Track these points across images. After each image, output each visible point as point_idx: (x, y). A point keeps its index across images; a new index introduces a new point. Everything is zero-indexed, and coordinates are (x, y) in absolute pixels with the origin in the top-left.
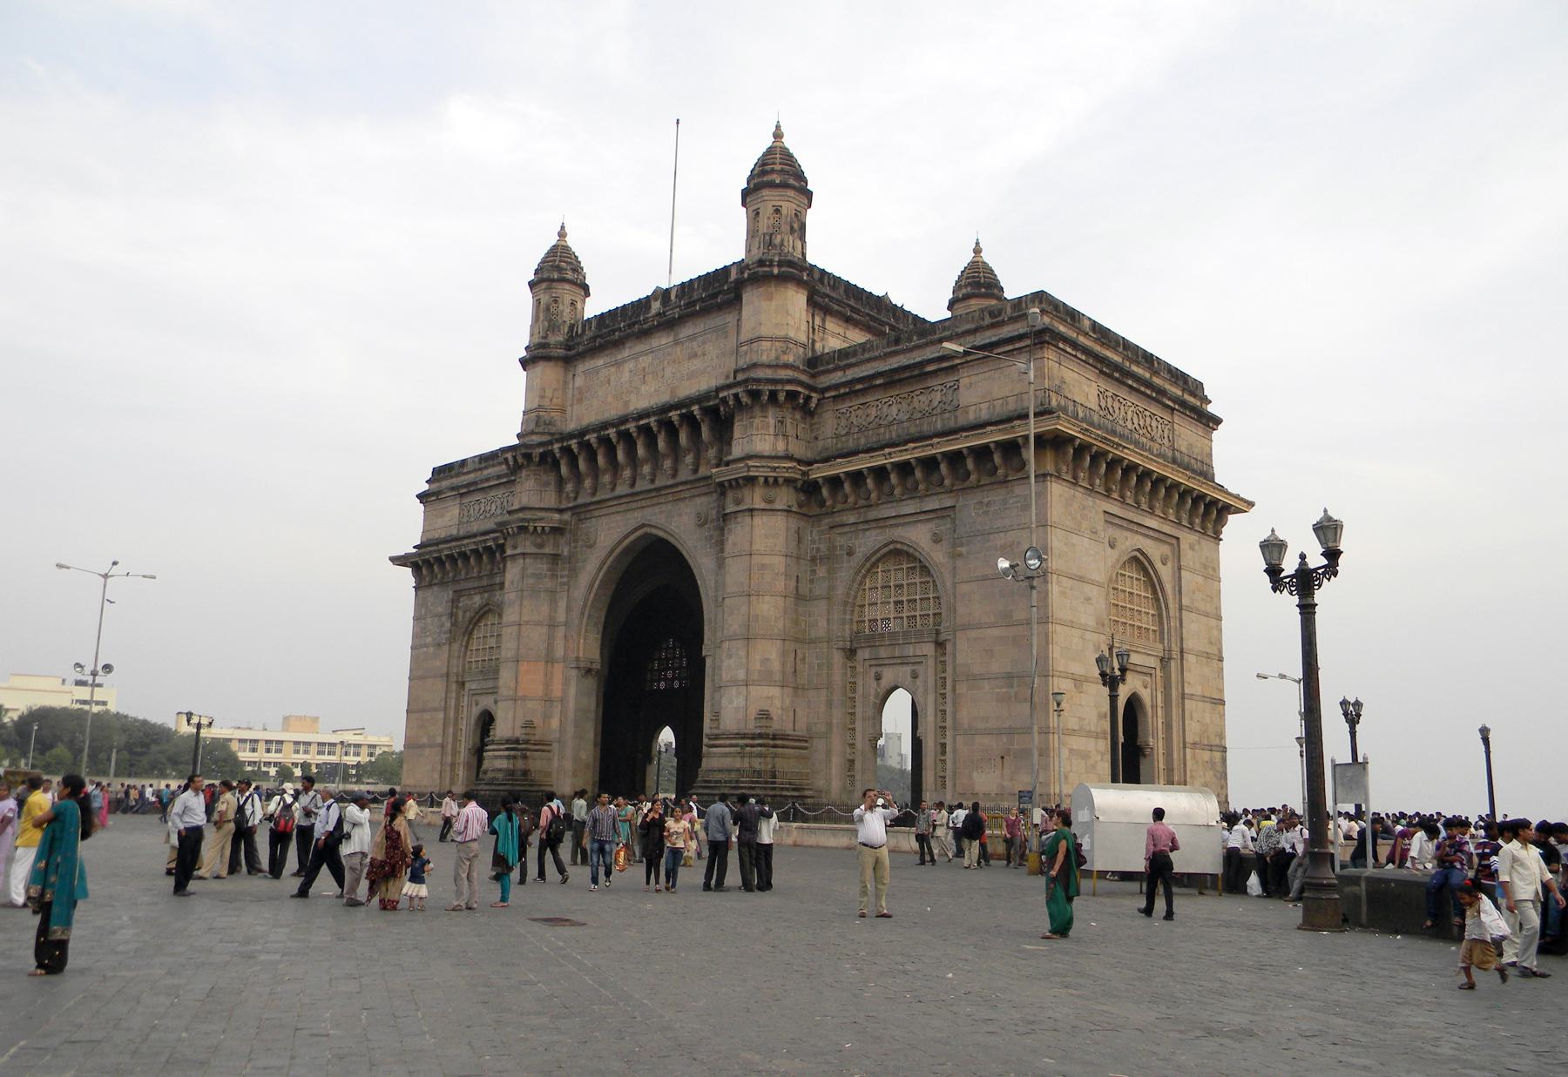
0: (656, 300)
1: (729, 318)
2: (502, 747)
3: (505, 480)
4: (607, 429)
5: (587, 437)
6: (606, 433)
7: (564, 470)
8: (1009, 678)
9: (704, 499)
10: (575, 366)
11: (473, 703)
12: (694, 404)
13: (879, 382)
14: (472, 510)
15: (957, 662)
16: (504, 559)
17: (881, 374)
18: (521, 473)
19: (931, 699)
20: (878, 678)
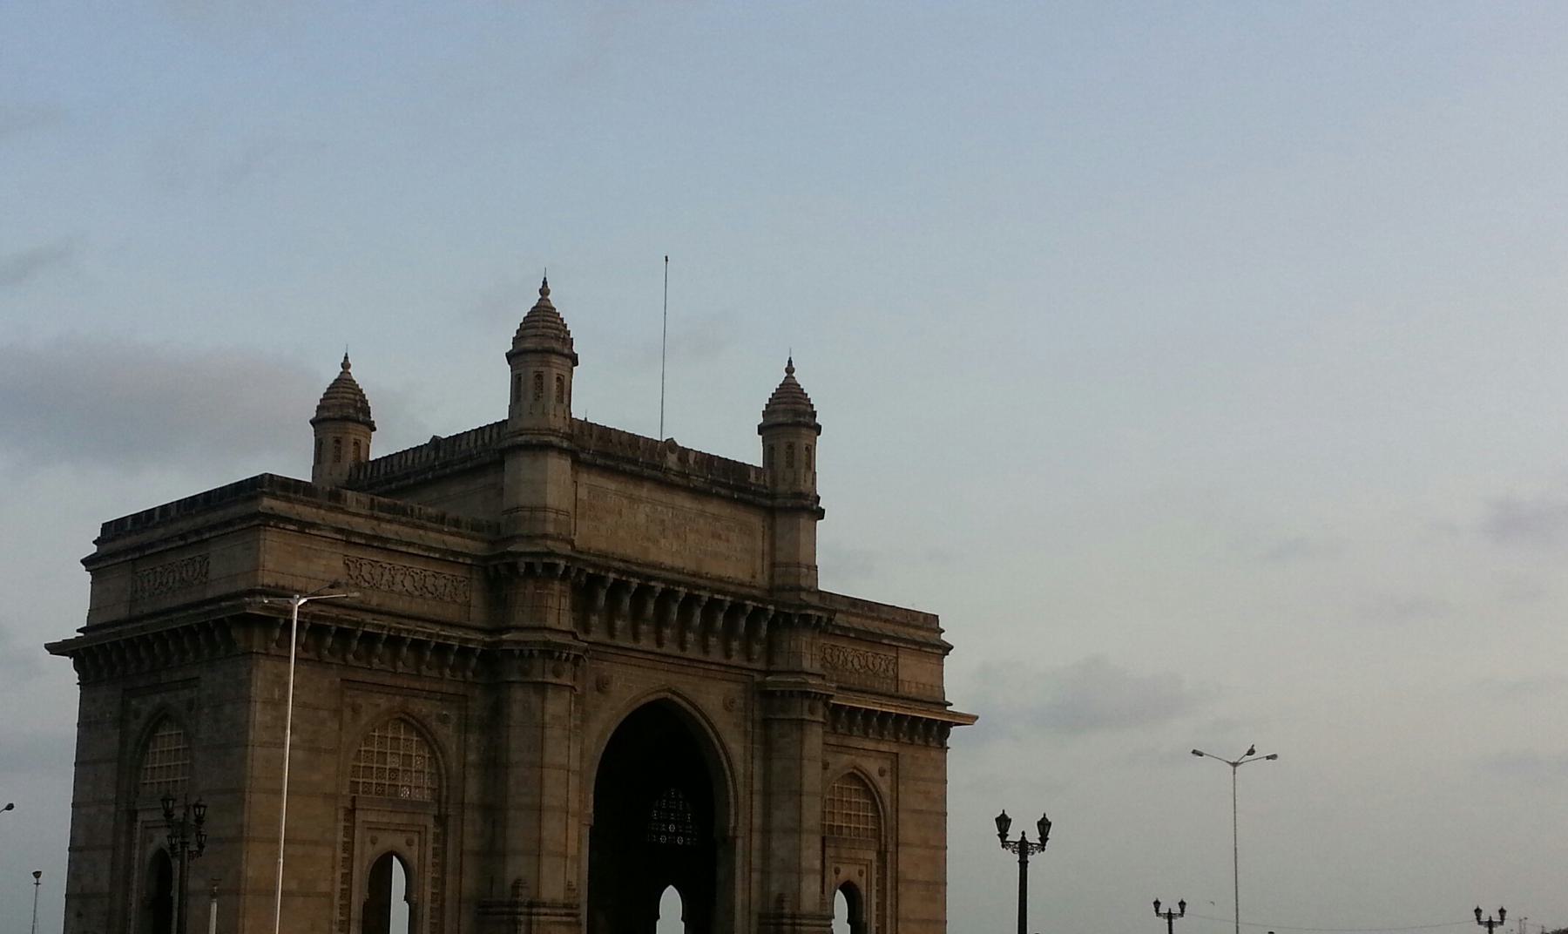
0: (672, 451)
1: (756, 521)
2: (558, 911)
3: (437, 556)
4: (679, 584)
5: (653, 583)
6: (677, 589)
7: (602, 600)
8: (928, 883)
9: (732, 686)
10: (577, 473)
11: (368, 839)
12: (770, 604)
13: (852, 635)
14: (366, 569)
15: (899, 869)
16: (541, 688)
17: (856, 630)
18: (553, 584)
19: (874, 892)
20: (837, 871)
